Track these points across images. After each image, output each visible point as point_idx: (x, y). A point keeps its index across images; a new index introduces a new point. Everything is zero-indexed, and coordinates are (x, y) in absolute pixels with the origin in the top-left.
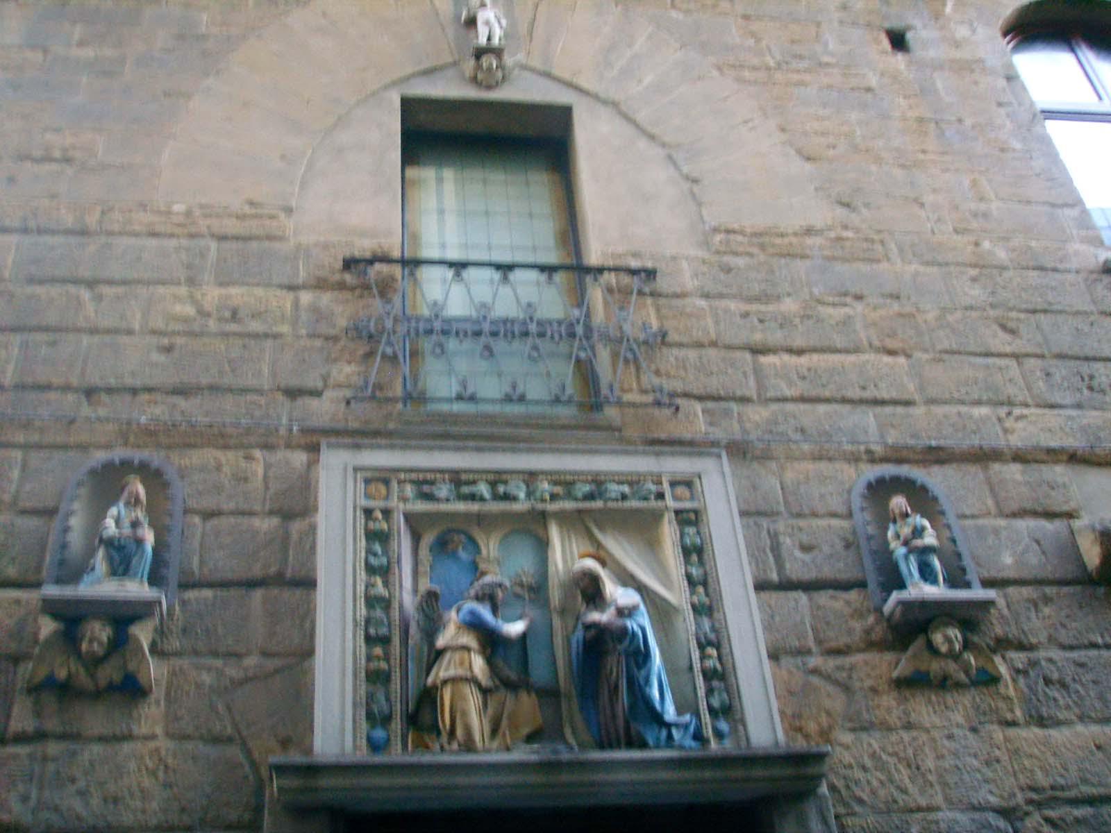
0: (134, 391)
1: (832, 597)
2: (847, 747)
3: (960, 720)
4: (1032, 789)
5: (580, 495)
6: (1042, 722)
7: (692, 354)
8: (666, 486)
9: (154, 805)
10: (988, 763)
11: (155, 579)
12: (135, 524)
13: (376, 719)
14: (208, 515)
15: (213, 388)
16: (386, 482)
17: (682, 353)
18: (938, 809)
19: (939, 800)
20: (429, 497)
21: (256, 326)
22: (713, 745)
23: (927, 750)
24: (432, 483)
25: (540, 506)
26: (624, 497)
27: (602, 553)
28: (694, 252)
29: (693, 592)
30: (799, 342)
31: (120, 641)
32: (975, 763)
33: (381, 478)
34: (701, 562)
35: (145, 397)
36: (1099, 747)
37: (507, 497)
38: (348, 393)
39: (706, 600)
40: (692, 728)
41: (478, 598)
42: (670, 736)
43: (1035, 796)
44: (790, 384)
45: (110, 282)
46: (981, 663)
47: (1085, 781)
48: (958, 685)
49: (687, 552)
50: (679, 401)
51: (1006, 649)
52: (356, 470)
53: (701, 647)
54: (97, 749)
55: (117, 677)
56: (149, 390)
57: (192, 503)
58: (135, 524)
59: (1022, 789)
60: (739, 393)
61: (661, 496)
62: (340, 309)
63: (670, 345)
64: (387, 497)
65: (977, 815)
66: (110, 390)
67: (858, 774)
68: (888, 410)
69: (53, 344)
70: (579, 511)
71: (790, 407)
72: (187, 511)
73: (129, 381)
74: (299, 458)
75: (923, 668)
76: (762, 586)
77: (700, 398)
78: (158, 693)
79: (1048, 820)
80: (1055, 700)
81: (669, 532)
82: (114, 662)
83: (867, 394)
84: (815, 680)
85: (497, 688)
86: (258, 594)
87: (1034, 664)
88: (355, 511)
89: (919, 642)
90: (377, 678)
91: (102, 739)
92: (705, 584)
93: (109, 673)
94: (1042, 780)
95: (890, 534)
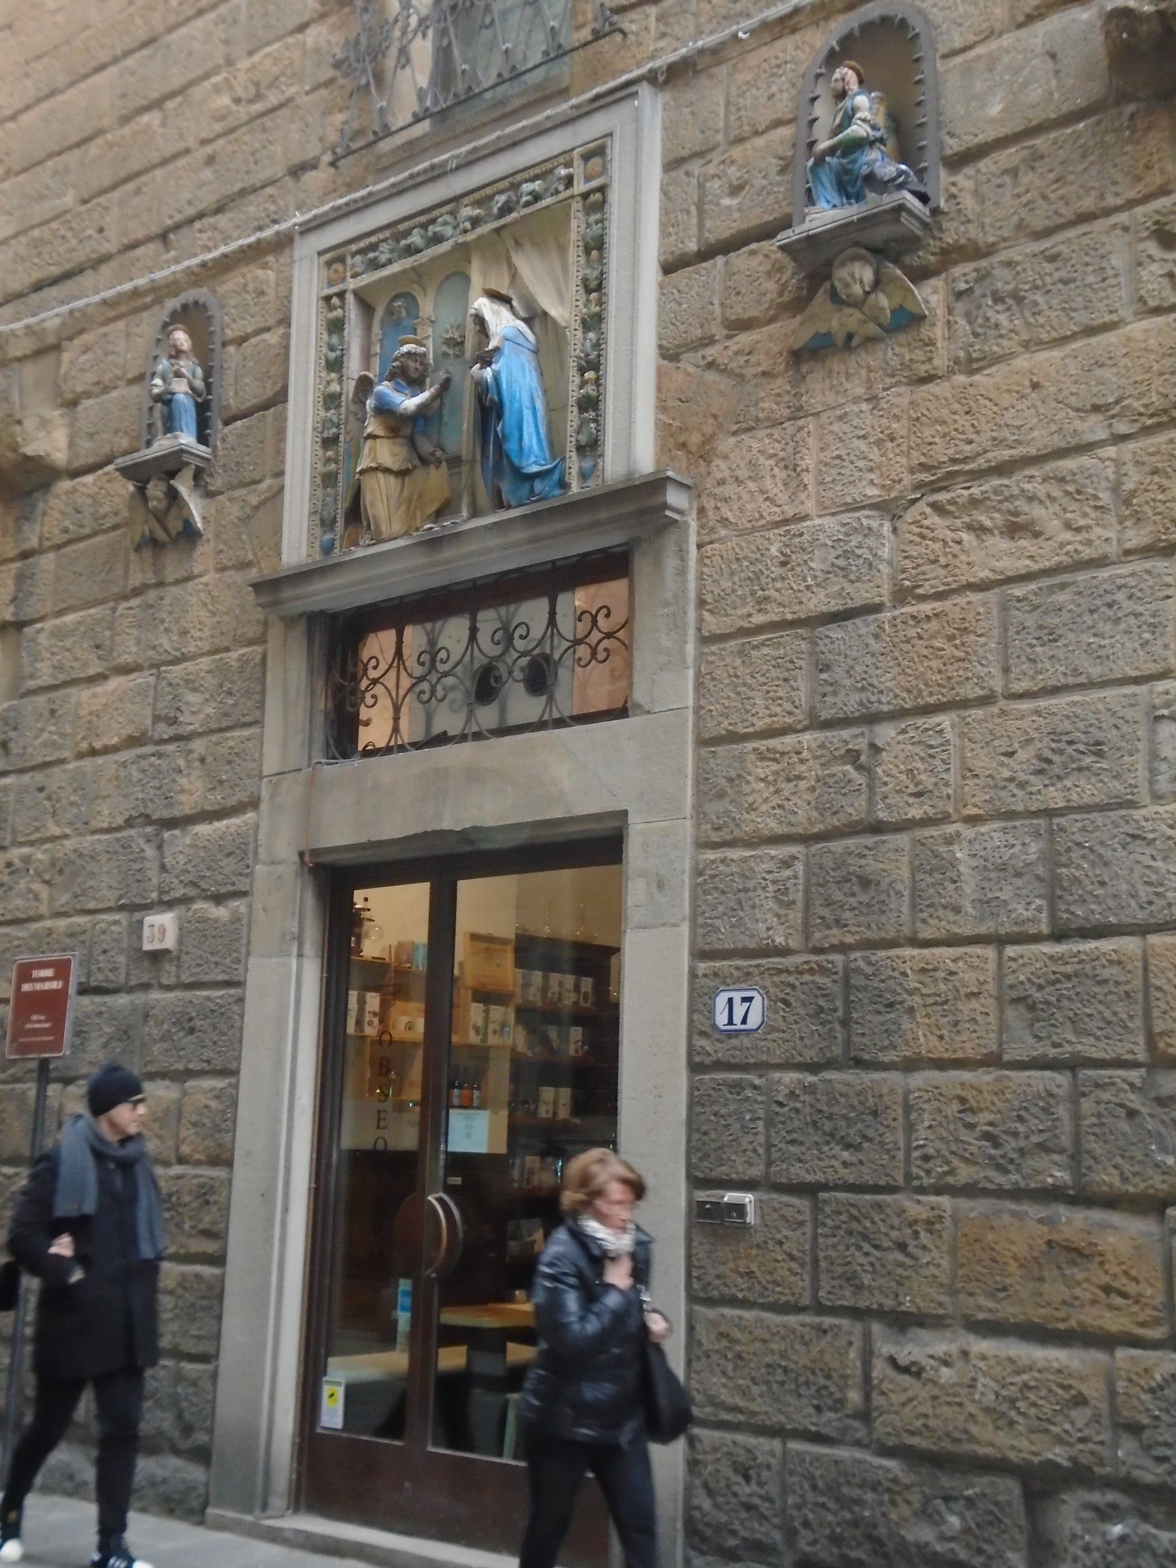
0: (190, 221)
1: (753, 253)
2: (726, 457)
3: (860, 391)
4: (924, 467)
5: (495, 210)
6: (970, 365)
9: (207, 632)
10: (879, 443)
13: (327, 524)
14: (241, 341)
15: (243, 193)
16: (341, 259)
18: (805, 517)
19: (810, 506)
20: (375, 265)
22: (575, 488)
23: (811, 441)
24: (374, 247)
25: (461, 239)
26: (536, 197)
29: (587, 303)
31: (173, 495)
32: (862, 445)
33: (335, 257)
34: (601, 258)
36: (1035, 386)
37: (438, 239)
40: (556, 476)
41: (391, 377)
42: (532, 491)
43: (926, 477)
46: (897, 300)
47: (998, 442)
48: (870, 340)
49: (588, 251)
51: (956, 263)
52: (320, 254)
53: (582, 371)
54: (175, 590)
55: (180, 527)
59: (912, 471)
61: (569, 181)
64: (343, 279)
65: (846, 518)
66: (177, 227)
67: (729, 490)
69: (138, 192)
70: (498, 230)
75: (823, 330)
78: (208, 535)
79: (937, 507)
80: (997, 326)
81: (578, 226)
82: (173, 512)
84: (711, 376)
85: (415, 467)
87: (983, 276)
89: (821, 296)
90: (329, 480)
91: (177, 582)
92: (599, 288)
93: (175, 525)
94: (941, 452)
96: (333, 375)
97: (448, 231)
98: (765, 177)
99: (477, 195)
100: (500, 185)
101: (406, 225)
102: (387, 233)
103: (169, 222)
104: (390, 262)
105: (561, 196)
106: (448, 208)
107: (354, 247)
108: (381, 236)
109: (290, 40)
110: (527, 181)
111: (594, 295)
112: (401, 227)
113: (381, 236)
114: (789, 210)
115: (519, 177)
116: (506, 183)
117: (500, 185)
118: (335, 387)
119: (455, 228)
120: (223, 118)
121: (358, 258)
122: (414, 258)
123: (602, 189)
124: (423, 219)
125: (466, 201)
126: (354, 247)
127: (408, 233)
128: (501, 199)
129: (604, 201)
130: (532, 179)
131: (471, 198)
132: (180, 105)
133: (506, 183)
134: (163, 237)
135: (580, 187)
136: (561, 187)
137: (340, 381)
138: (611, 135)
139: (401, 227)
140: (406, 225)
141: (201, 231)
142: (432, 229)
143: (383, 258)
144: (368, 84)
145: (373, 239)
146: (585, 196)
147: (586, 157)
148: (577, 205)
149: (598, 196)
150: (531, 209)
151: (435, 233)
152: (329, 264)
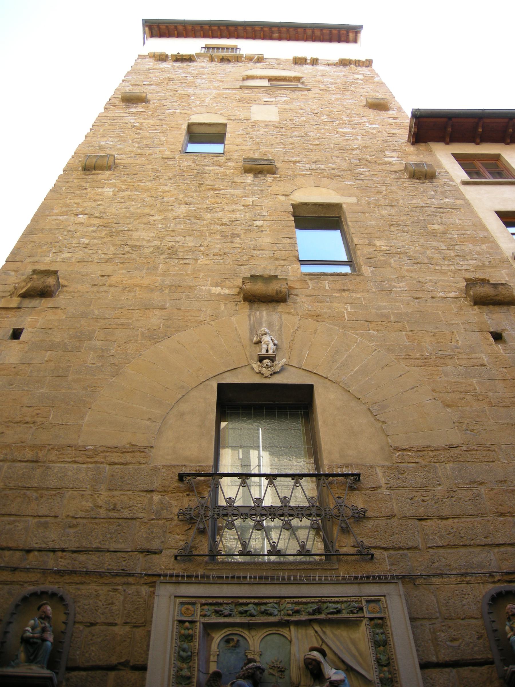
0: (54, 551)
1: (471, 671)
5: (311, 610)
7: (382, 523)
8: (364, 603)
11: (52, 665)
12: (44, 630)
15: (98, 550)
17: (376, 522)
21: (126, 513)
24: (221, 604)
27: (324, 647)
28: (383, 463)
29: (381, 671)
30: (446, 511)
35: (60, 554)
38: (176, 552)
39: (388, 675)
44: (441, 537)
45: (48, 489)
50: (373, 551)
52: (175, 596)
56: (63, 550)
57: (79, 618)
58: (44, 630)
60: (410, 544)
61: (361, 609)
62: (176, 503)
63: (369, 518)
68: (503, 549)
71: (441, 551)
72: (75, 622)
73: (51, 545)
74: (144, 590)
76: (425, 666)
77: (386, 549)
83: (489, 541)
86: (112, 674)
88: (173, 621)
92: (388, 665)
95: (507, 628)
96: (185, 666)
97: (276, 612)
98: (470, 638)
99: (296, 600)
100: (313, 600)
101: (244, 601)
102: (230, 601)
103: (36, 546)
104: (230, 615)
105: (355, 615)
106: (275, 600)
107: (204, 601)
108: (226, 601)
109: (141, 494)
110: (330, 602)
111: (386, 669)
112: (241, 601)
113: (226, 601)
114: (490, 656)
115: (325, 599)
116: (317, 599)
117: (313, 600)
118: (185, 672)
119: (280, 611)
120: (87, 511)
121: (206, 607)
122: (249, 618)
123: (381, 618)
124: (256, 601)
125: (288, 600)
126: (204, 601)
127: (247, 604)
128: (315, 606)
129: (383, 625)
130: (333, 602)
131: (292, 600)
132: (55, 495)
133: (317, 599)
134: (29, 551)
135: (367, 615)
136: (356, 611)
137: (189, 668)
138: (384, 596)
139: (241, 601)
140: (244, 601)
141: (61, 558)
142: (263, 608)
143: (227, 612)
144: (204, 528)
145: (220, 601)
146: (371, 619)
147: (368, 602)
148: (365, 622)
149: (380, 621)
150: (335, 616)
151: (265, 610)
152: (182, 603)
